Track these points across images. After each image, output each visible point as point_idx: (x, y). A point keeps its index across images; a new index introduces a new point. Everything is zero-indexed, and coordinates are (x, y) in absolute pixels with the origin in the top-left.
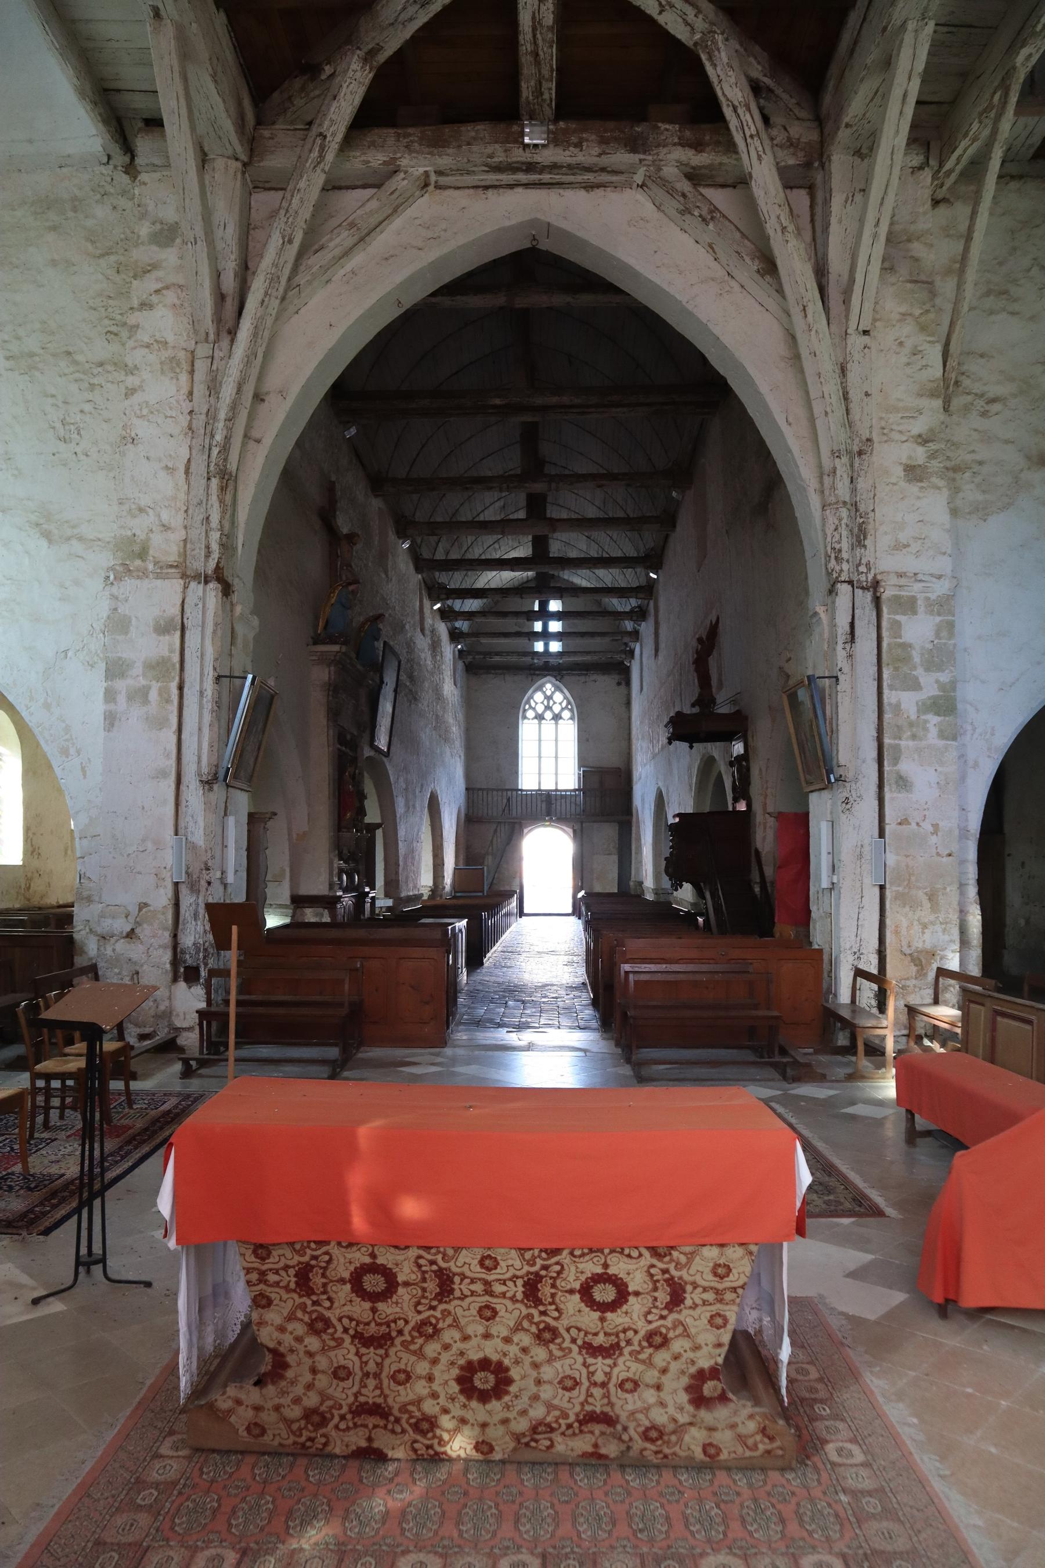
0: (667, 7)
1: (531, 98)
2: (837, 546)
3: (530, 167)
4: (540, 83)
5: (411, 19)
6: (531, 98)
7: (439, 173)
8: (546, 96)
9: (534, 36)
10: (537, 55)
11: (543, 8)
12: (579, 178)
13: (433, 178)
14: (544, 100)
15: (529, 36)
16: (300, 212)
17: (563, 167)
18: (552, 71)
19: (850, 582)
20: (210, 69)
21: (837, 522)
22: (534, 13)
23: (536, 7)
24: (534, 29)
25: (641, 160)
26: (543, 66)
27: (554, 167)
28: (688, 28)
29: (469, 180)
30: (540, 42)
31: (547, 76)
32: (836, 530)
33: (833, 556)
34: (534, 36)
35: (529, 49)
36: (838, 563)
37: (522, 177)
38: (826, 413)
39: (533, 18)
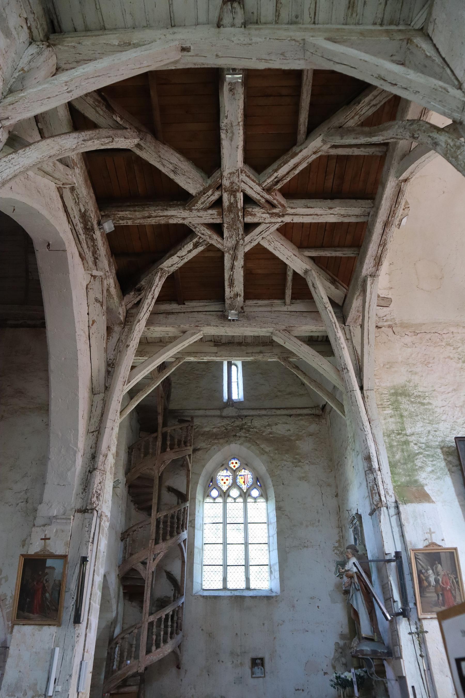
1: (119, 216)
2: (99, 492)
3: (88, 230)
5: (164, 165)
8: (121, 222)
9: (161, 216)
10: (149, 217)
12: (86, 250)
14: (118, 221)
15: (161, 214)
17: (94, 243)
19: (97, 511)
21: (101, 480)
23: (180, 217)
24: (166, 216)
25: (108, 271)
27: (93, 240)
28: (170, 265)
29: (70, 204)
31: (136, 222)
32: (100, 483)
33: (96, 495)
34: (161, 216)
36: (97, 500)
37: (80, 227)
38: (112, 429)
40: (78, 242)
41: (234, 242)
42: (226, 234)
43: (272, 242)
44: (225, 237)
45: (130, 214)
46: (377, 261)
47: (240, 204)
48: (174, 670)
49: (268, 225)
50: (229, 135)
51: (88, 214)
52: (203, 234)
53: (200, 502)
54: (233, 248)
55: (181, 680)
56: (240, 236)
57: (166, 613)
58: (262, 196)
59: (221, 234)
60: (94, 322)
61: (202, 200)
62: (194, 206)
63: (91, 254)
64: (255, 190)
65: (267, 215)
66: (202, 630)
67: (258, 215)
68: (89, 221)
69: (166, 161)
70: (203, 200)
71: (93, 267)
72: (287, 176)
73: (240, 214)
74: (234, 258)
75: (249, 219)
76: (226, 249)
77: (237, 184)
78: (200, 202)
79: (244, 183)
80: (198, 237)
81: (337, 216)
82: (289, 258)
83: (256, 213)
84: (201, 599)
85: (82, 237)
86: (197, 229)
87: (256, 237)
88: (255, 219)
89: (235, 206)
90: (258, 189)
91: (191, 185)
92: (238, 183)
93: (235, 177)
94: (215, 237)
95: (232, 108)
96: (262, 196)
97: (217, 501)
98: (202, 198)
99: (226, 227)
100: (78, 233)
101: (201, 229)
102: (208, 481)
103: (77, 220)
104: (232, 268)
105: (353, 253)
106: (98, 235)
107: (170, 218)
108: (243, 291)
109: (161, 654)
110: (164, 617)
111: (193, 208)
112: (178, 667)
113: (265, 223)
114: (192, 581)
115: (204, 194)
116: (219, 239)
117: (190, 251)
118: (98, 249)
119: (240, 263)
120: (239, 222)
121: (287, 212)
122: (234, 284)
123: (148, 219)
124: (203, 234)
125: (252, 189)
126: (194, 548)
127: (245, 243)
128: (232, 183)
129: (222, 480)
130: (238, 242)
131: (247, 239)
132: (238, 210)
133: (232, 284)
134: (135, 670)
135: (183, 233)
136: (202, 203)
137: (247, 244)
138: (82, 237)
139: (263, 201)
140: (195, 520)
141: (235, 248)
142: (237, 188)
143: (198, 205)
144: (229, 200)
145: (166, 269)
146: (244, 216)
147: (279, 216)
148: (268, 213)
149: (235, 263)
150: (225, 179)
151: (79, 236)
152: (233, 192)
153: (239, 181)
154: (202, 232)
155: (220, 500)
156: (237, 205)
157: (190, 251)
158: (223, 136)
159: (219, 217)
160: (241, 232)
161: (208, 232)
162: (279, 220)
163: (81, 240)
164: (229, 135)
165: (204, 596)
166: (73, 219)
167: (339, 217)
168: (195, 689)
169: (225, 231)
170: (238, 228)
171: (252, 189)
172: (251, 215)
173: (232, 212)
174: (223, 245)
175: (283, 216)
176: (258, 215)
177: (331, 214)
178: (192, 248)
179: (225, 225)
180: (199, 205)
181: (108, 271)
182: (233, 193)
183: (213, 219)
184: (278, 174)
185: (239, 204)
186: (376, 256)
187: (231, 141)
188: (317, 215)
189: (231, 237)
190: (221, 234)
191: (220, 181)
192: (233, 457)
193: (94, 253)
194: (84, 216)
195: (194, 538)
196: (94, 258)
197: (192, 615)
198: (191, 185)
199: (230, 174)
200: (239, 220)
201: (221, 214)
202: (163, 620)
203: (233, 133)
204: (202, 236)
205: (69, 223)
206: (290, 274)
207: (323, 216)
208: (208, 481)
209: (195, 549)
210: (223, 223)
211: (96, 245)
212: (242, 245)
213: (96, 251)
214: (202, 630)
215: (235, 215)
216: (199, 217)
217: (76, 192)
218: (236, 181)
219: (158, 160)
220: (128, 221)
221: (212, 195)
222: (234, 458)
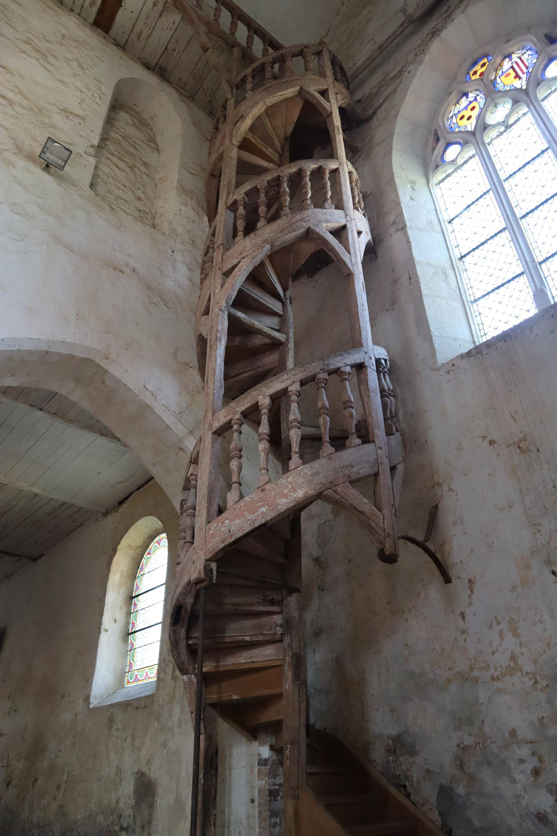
48: (434, 591)
53: (413, 183)
55: (463, 615)
57: (271, 391)
66: (492, 443)
84: (465, 363)
97: (460, 161)
102: (427, 141)
109: (264, 509)
110: (265, 402)
112: (448, 580)
114: (428, 337)
126: (414, 266)
129: (462, 117)
134: (186, 580)
140: (401, 214)
155: (471, 151)
165: (469, 352)
168: (516, 635)
192: (470, 61)
195: (410, 249)
197: (450, 420)
202: (265, 411)
208: (427, 141)
209: (418, 267)
214: (492, 443)
222: (475, 63)
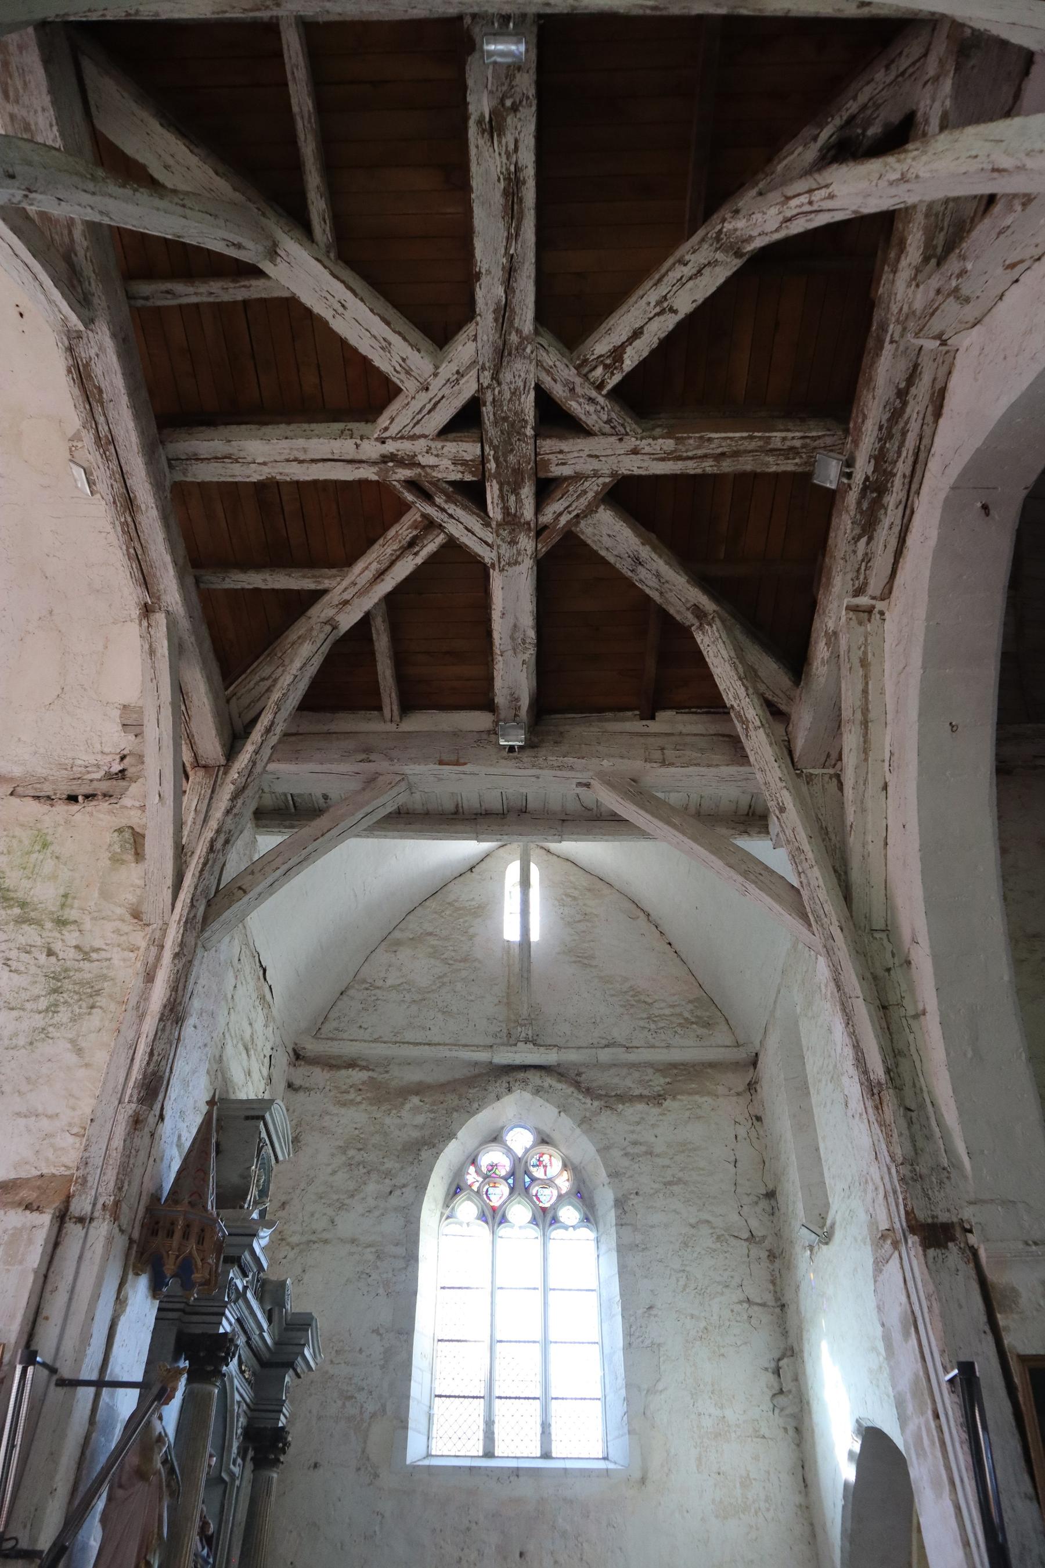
0: (665, 305)
1: (797, 461)
3: (876, 488)
4: (772, 450)
5: (658, 575)
6: (797, 461)
7: (859, 592)
10: (723, 454)
11: (647, 449)
12: (914, 427)
13: (863, 601)
14: (804, 446)
15: (690, 464)
16: (769, 779)
17: (882, 448)
18: (751, 438)
20: (655, 765)
22: (654, 459)
23: (646, 457)
24: (680, 458)
25: (891, 342)
26: (742, 448)
27: (880, 458)
28: (706, 271)
29: (882, 562)
30: (700, 452)
31: (760, 443)
35: (713, 463)
37: (893, 498)
39: (663, 459)
40: (922, 456)
41: (507, 376)
42: (529, 401)
43: (398, 368)
44: (532, 394)
45: (767, 464)
46: (89, 386)
47: (492, 492)
49: (417, 430)
50: (519, 635)
51: (858, 531)
52: (591, 400)
54: (510, 354)
56: (489, 397)
58: (443, 510)
59: (544, 400)
60: (1012, 266)
61: (583, 502)
62: (604, 484)
63: (908, 410)
64: (462, 525)
65: (424, 460)
67: (447, 461)
68: (862, 512)
69: (650, 583)
70: (582, 500)
71: (925, 362)
72: (394, 558)
73: (492, 466)
74: (504, 313)
75: (470, 450)
76: (528, 350)
77: (503, 540)
78: (590, 495)
79: (486, 543)
80: (604, 392)
81: (249, 459)
82: (341, 310)
83: (452, 467)
85: (902, 468)
86: (605, 417)
87: (446, 391)
88: (454, 450)
89: (506, 487)
90: (455, 530)
91: (605, 531)
92: (499, 542)
93: (507, 555)
94: (558, 391)
95: (513, 675)
96: (443, 510)
98: (582, 507)
99: (529, 427)
100: (907, 480)
101: (594, 417)
103: (891, 516)
104: (510, 272)
105: (147, 298)
106: (863, 468)
107: (672, 452)
108: (473, 151)
111: (607, 480)
113: (425, 436)
115: (577, 516)
116: (547, 381)
117: (637, 334)
118: (881, 428)
119: (488, 293)
120: (495, 442)
121: (375, 469)
122: (506, 193)
123: (725, 450)
124: (591, 400)
125: (466, 528)
127: (474, 373)
128: (513, 542)
130: (495, 377)
131: (468, 388)
132: (497, 475)
133: (513, 183)
135: (643, 396)
136: (585, 492)
137: (469, 368)
138: (902, 468)
139: (439, 500)
141: (502, 354)
142: (501, 531)
143: (595, 488)
144: (519, 500)
145: (719, 256)
146: (483, 459)
147: (392, 457)
148: (423, 467)
149: (500, 291)
150: (529, 552)
151: (908, 473)
152: (511, 521)
153: (499, 547)
154: (591, 408)
156: (501, 490)
157: (637, 334)
158: (532, 634)
159: (547, 457)
160: (488, 412)
161: (576, 408)
162: (390, 447)
163: (910, 460)
164: (519, 635)
166: (898, 522)
167: (242, 454)
169: (532, 414)
170: (496, 423)
171: (466, 528)
172: (465, 463)
173: (514, 470)
174: (539, 364)
175: (385, 459)
176: (446, 463)
177: (265, 464)
178: (629, 349)
179: (529, 432)
180: (593, 487)
181: (891, 342)
182: (510, 518)
183: (561, 452)
184: (415, 562)
185: (496, 492)
186: (101, 402)
187: (515, 626)
188: (301, 462)
189: (513, 393)
190: (544, 400)
191: (540, 546)
193: (896, 414)
194: (868, 525)
196: (907, 393)
198: (605, 531)
199: (516, 563)
200: (495, 448)
201: (540, 464)
203: (512, 638)
204: (594, 394)
205: (912, 512)
206: (322, 230)
207: (283, 457)
210: (536, 436)
211: (880, 440)
212: (483, 368)
213: (888, 420)
215: (506, 461)
216: (597, 457)
217: (853, 585)
218: (504, 546)
219: (667, 585)
220: (779, 445)
221: (561, 514)
